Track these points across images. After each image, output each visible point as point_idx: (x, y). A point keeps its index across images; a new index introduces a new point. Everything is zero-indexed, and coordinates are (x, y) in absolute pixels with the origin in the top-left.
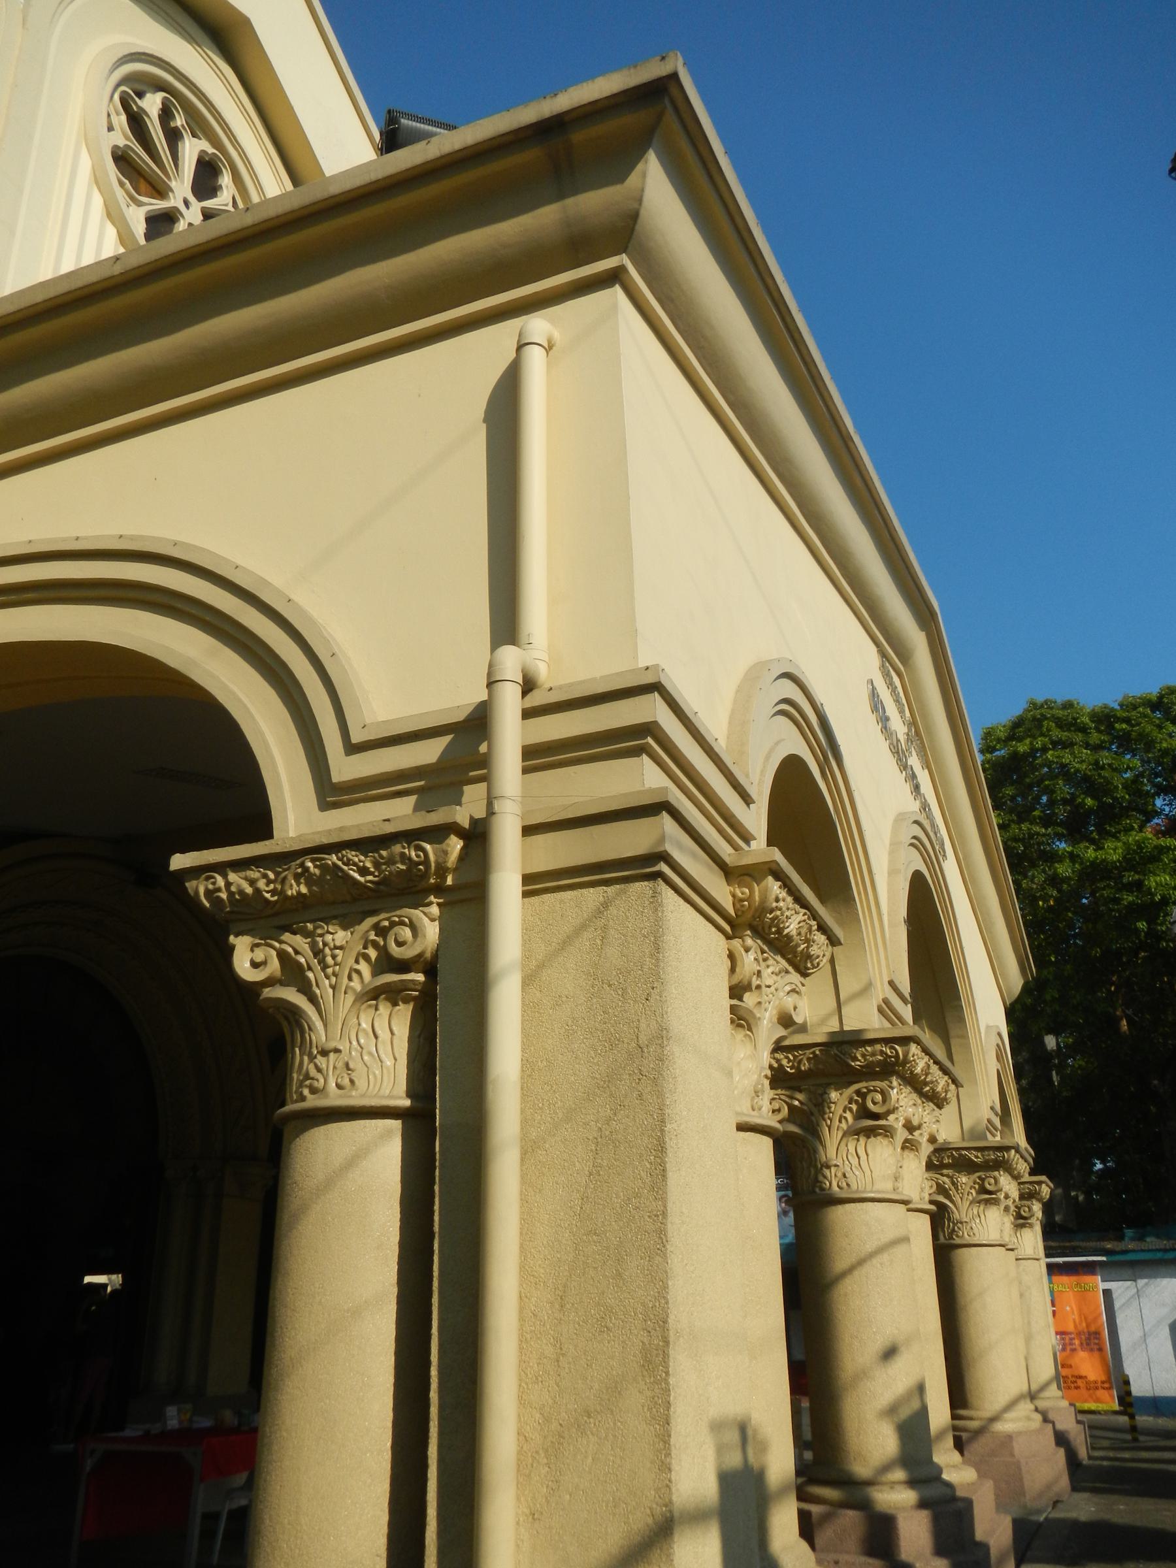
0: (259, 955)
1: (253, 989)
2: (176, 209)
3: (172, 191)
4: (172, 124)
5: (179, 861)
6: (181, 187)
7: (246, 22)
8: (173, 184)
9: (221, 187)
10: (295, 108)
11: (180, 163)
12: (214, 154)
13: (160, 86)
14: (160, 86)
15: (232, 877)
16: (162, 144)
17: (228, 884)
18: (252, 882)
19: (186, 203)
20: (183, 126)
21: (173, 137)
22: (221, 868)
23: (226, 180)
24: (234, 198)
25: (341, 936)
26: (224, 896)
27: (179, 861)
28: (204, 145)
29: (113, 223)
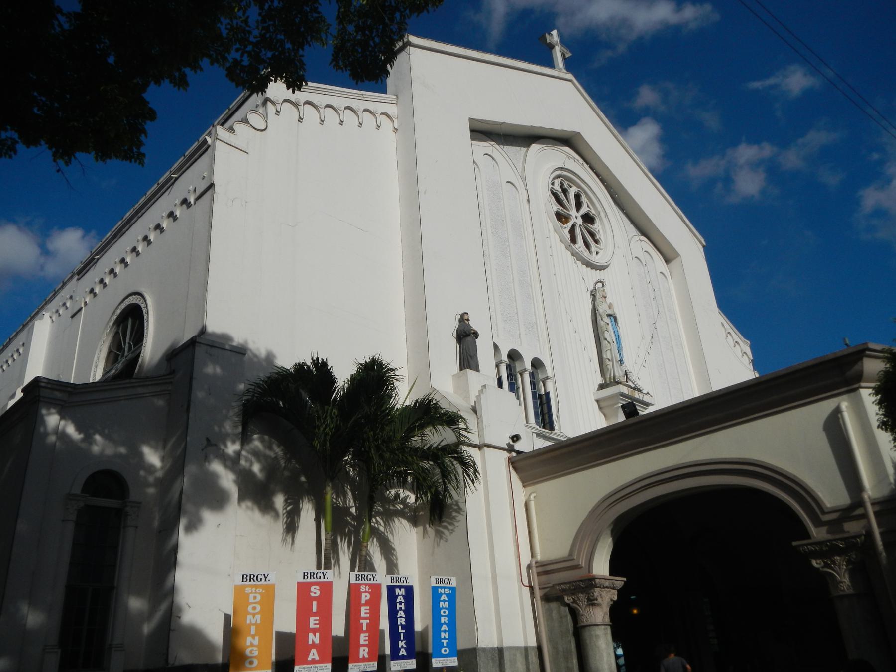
0: (818, 562)
1: (818, 569)
3: (571, 215)
5: (794, 543)
6: (573, 212)
8: (571, 213)
9: (582, 201)
11: (569, 199)
15: (809, 546)
17: (808, 548)
18: (814, 547)
21: (565, 191)
22: (807, 545)
23: (584, 199)
25: (838, 558)
26: (807, 550)
27: (794, 543)
29: (563, 243)
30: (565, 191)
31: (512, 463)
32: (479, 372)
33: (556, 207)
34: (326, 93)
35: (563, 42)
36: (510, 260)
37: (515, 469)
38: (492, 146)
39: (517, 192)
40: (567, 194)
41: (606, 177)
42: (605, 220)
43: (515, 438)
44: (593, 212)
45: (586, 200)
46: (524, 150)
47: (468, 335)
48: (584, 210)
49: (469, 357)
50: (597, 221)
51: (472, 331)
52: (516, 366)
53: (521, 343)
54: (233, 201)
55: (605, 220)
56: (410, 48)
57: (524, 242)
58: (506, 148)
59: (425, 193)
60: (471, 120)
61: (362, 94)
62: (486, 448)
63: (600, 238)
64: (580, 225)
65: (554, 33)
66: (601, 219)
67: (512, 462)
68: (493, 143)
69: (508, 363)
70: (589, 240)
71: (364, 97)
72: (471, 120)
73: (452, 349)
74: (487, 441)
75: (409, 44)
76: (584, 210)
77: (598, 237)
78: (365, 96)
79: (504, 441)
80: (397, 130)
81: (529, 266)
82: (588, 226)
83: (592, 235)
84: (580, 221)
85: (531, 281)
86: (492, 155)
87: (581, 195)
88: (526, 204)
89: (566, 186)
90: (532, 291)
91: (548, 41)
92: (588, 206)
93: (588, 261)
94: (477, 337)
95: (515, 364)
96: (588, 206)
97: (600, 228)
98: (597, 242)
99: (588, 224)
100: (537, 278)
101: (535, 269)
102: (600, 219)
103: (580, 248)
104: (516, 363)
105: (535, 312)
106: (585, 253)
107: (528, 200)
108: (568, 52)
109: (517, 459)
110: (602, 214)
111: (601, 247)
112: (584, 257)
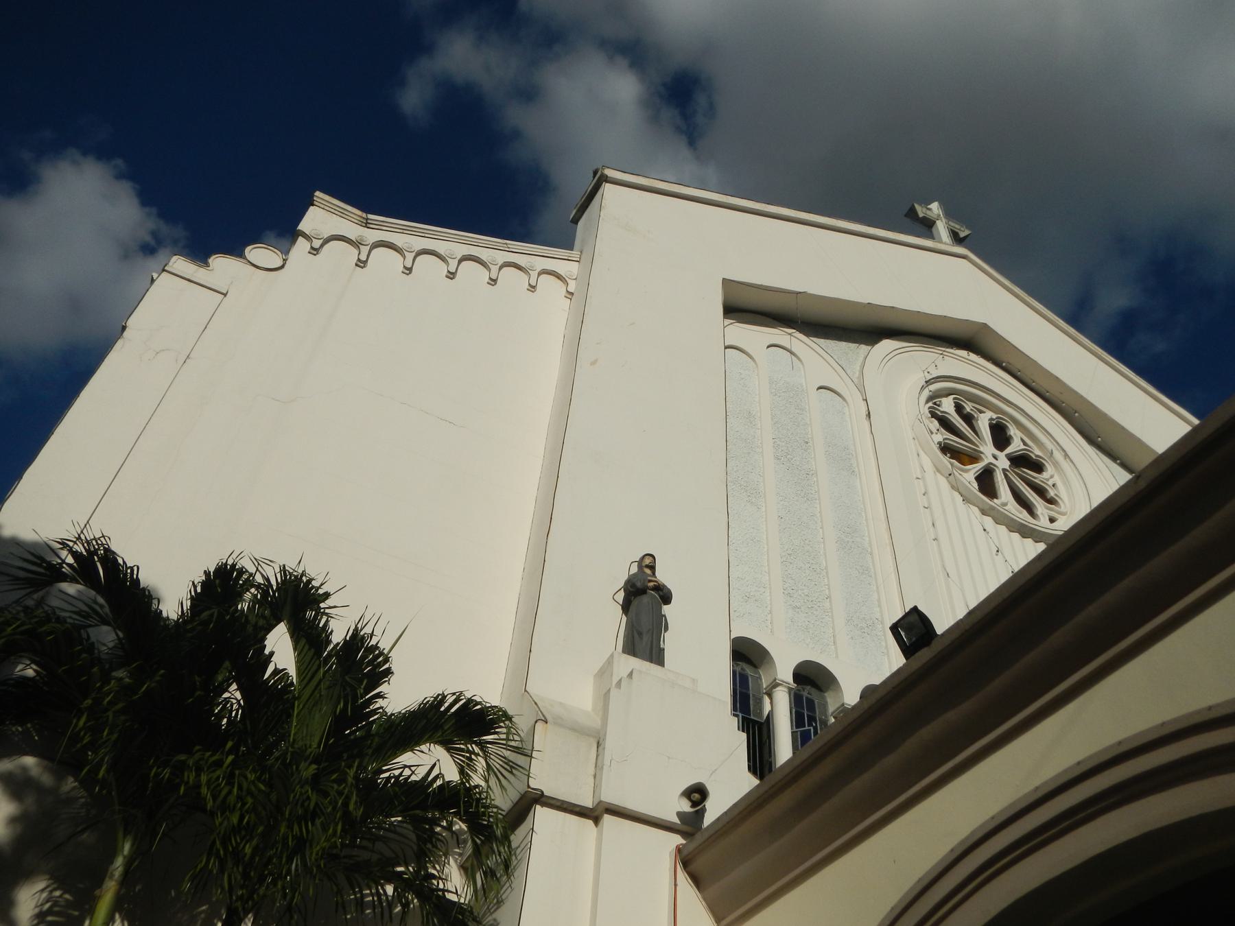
2: (991, 463)
3: (982, 453)
4: (965, 412)
6: (988, 449)
7: (985, 326)
8: (981, 449)
9: (1010, 436)
10: (1039, 362)
11: (979, 433)
12: (998, 418)
13: (948, 393)
14: (948, 393)
16: (964, 428)
19: (995, 457)
20: (971, 410)
21: (969, 419)
23: (1013, 431)
24: (1022, 440)
28: (989, 415)
30: (969, 419)
31: (685, 864)
32: (664, 666)
33: (942, 436)
34: (427, 235)
35: (949, 214)
36: (818, 506)
37: (696, 880)
38: (790, 334)
39: (846, 405)
40: (974, 422)
41: (1054, 392)
42: (1065, 465)
43: (696, 796)
44: (1038, 452)
45: (1017, 432)
46: (869, 348)
47: (642, 591)
48: (1015, 446)
49: (636, 635)
50: (1050, 470)
51: (651, 584)
52: (827, 702)
53: (837, 654)
54: (157, 353)
55: (1065, 465)
56: (607, 184)
57: (858, 480)
58: (822, 341)
59: (594, 363)
60: (727, 283)
61: (506, 244)
62: (607, 818)
63: (1056, 495)
64: (1004, 470)
65: (935, 206)
66: (1056, 465)
67: (686, 860)
68: (790, 331)
69: (794, 685)
70: (1030, 497)
71: (509, 248)
72: (727, 283)
73: (614, 622)
74: (611, 796)
75: (604, 179)
76: (1015, 446)
77: (1052, 493)
78: (509, 246)
79: (673, 807)
80: (572, 294)
81: (866, 520)
82: (1024, 472)
83: (1040, 491)
84: (1003, 463)
85: (871, 546)
86: (788, 346)
87: (1007, 426)
88: (866, 423)
89: (968, 410)
90: (873, 562)
91: (921, 215)
92: (1025, 444)
93: (1022, 524)
94: (666, 598)
95: (824, 698)
96: (1025, 444)
97: (1057, 479)
98: (1051, 501)
99: (1025, 470)
100: (888, 541)
101: (884, 525)
102: (1054, 464)
103: (1005, 504)
104: (826, 694)
105: (879, 601)
106: (1022, 515)
107: (869, 415)
108: (962, 229)
109: (692, 846)
110: (1058, 455)
111: (1063, 509)
112: (1017, 519)
